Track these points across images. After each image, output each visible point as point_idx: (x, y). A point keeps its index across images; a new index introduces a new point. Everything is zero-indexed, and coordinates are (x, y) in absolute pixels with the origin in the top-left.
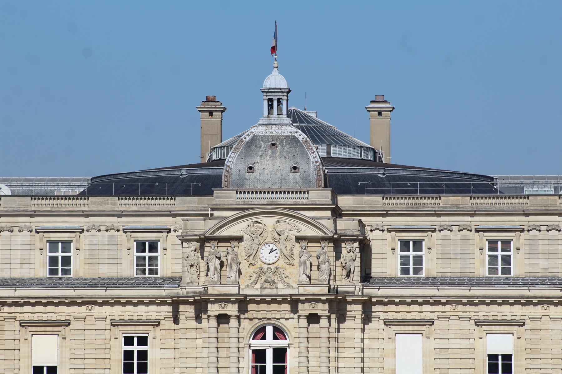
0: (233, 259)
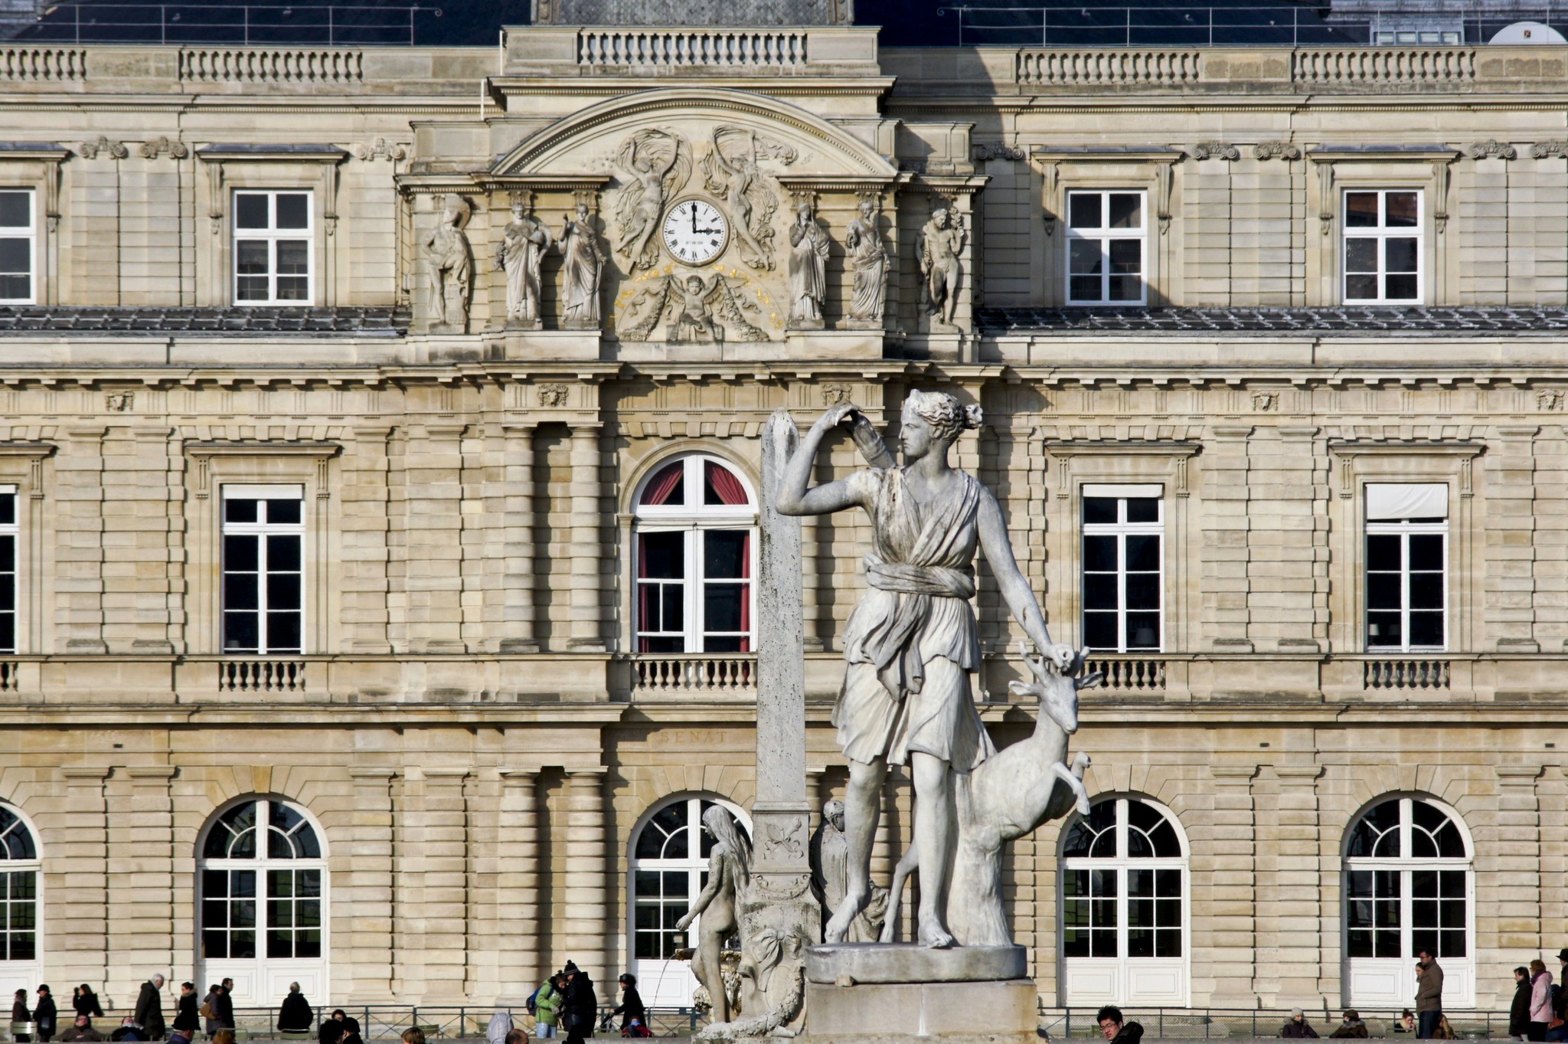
0: (582, 250)
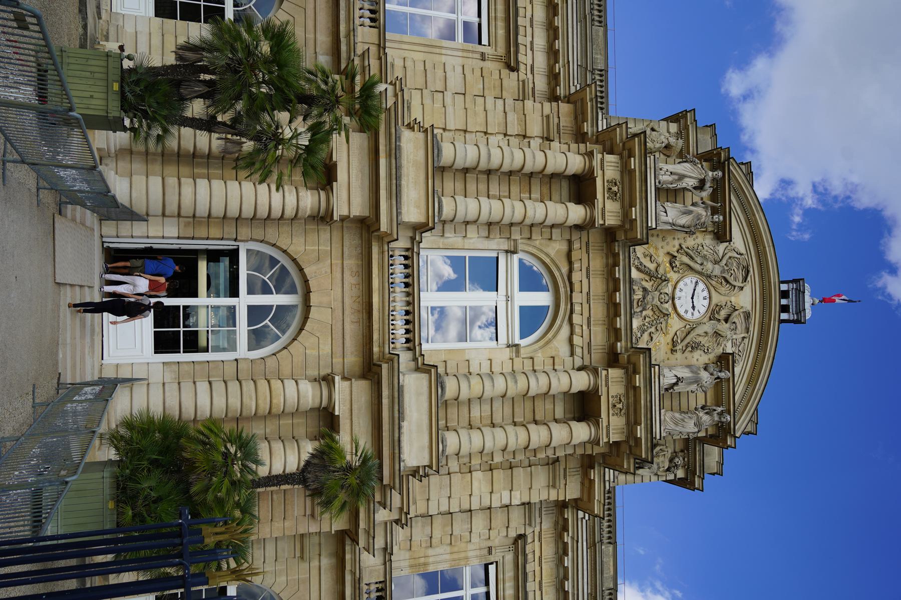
0: (699, 217)
